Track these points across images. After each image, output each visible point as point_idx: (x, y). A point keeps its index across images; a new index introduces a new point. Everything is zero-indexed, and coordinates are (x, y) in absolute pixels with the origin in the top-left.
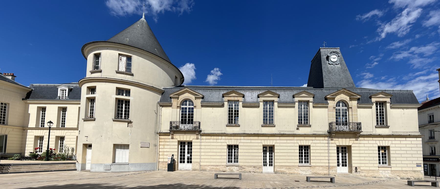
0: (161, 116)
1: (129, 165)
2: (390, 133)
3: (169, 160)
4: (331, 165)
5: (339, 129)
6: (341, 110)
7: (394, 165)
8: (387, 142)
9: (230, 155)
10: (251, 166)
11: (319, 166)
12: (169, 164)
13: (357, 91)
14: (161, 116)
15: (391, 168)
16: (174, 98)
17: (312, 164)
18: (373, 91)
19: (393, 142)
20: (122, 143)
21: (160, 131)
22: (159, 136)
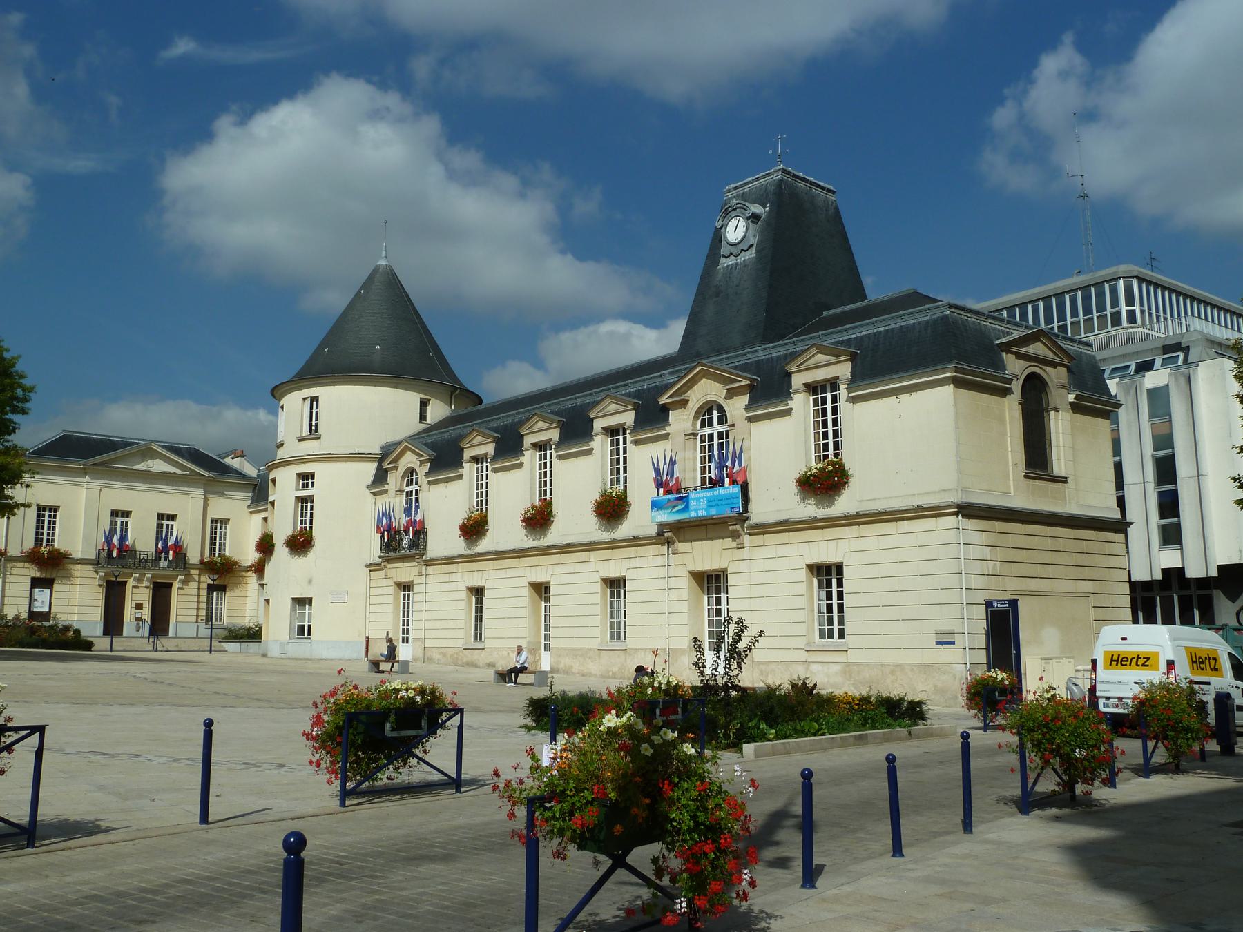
15: (847, 651)
16: (391, 469)
17: (630, 643)
19: (854, 545)
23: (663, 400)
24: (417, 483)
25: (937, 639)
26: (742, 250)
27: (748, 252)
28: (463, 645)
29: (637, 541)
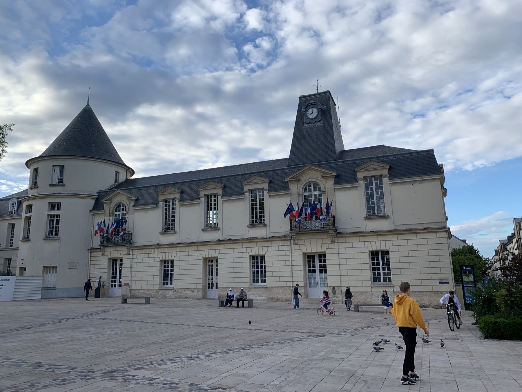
0: (93, 227)
1: (57, 290)
3: (96, 283)
5: (300, 227)
6: (313, 196)
8: (383, 243)
10: (187, 289)
11: (278, 287)
12: (96, 288)
14: (93, 227)
17: (268, 284)
19: (395, 243)
20: (50, 264)
21: (91, 247)
23: (288, 179)
24: (126, 210)
25: (439, 281)
27: (319, 123)
28: (158, 288)
29: (272, 239)
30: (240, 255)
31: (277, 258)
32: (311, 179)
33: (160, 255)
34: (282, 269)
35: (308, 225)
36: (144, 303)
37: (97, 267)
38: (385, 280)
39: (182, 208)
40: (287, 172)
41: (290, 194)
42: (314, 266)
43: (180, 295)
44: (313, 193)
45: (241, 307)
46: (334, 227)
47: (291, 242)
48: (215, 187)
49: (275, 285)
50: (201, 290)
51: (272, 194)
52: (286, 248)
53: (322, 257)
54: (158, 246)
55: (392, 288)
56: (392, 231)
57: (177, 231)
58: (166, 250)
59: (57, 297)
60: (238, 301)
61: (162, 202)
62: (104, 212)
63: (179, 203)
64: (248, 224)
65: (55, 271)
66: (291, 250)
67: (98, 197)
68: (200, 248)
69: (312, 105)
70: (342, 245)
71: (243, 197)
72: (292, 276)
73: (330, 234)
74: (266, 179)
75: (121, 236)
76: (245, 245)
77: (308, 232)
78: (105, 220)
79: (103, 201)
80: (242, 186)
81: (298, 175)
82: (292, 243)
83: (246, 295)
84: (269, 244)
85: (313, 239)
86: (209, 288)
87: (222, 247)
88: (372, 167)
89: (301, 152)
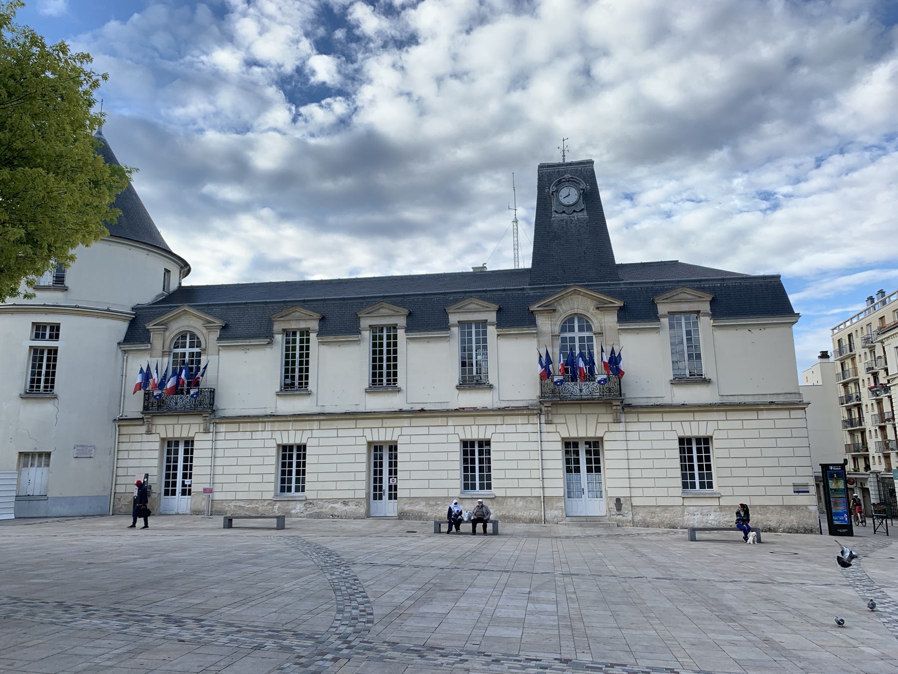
0: (124, 377)
2: (716, 400)
4: (548, 493)
6: (577, 340)
7: (728, 491)
9: (285, 474)
10: (336, 501)
11: (516, 497)
13: (618, 286)
17: (494, 492)
18: (665, 284)
19: (722, 425)
21: (121, 415)
22: (117, 428)
23: (534, 308)
26: (574, 211)
27: (580, 214)
30: (443, 439)
31: (513, 446)
32: (576, 310)
33: (277, 435)
34: (522, 465)
35: (574, 390)
36: (275, 526)
37: (133, 455)
38: (702, 486)
39: (324, 348)
40: (531, 294)
41: (537, 335)
42: (577, 461)
43: (320, 510)
44: (577, 334)
45: (480, 534)
46: (620, 395)
47: (540, 418)
48: (393, 313)
49: (510, 493)
50: (363, 501)
51: (504, 331)
52: (530, 428)
53: (595, 446)
54: (274, 418)
55: (718, 499)
56: (715, 405)
57: (313, 391)
58: (290, 426)
59: (49, 515)
60: (474, 523)
61: (281, 335)
62: (151, 347)
63: (319, 338)
64: (457, 383)
65: (43, 463)
66: (541, 432)
67: (136, 316)
68: (362, 423)
69: (568, 181)
70: (632, 427)
71: (448, 333)
72: (543, 478)
73: (615, 408)
74: (493, 305)
75: (192, 396)
76: (451, 421)
77: (577, 402)
78: (148, 365)
79: (149, 326)
80: (446, 315)
81: (554, 301)
82: (543, 421)
83: (488, 513)
84: (499, 420)
85: (581, 414)
86: (375, 498)
87: (406, 422)
88: (682, 296)
89: (553, 262)
